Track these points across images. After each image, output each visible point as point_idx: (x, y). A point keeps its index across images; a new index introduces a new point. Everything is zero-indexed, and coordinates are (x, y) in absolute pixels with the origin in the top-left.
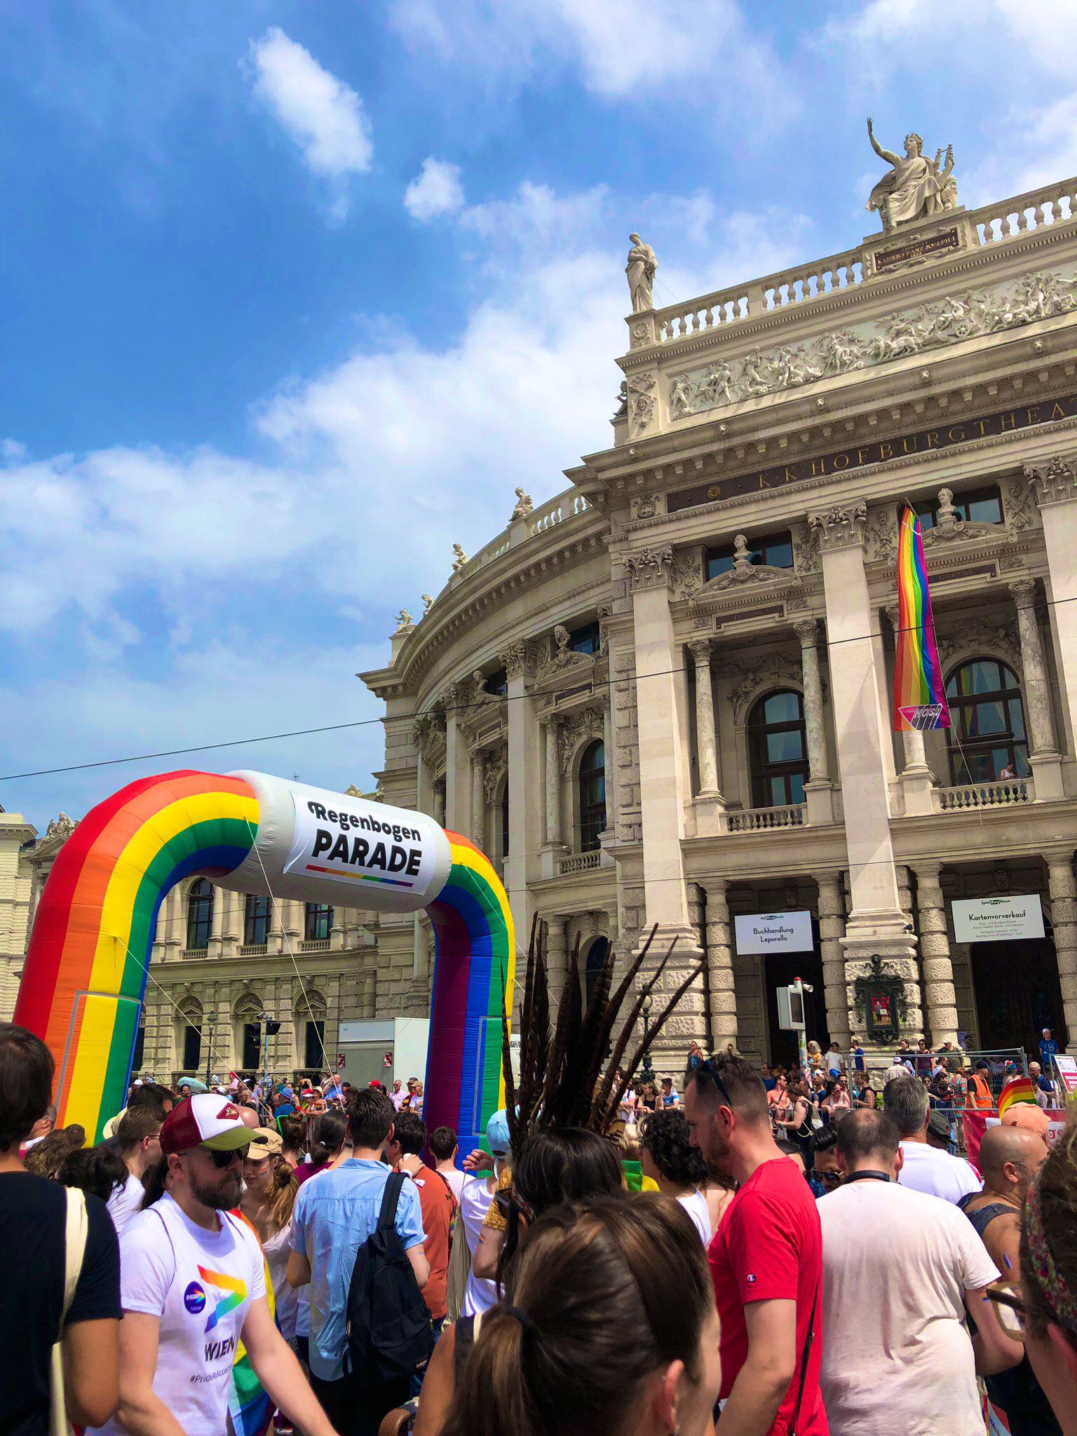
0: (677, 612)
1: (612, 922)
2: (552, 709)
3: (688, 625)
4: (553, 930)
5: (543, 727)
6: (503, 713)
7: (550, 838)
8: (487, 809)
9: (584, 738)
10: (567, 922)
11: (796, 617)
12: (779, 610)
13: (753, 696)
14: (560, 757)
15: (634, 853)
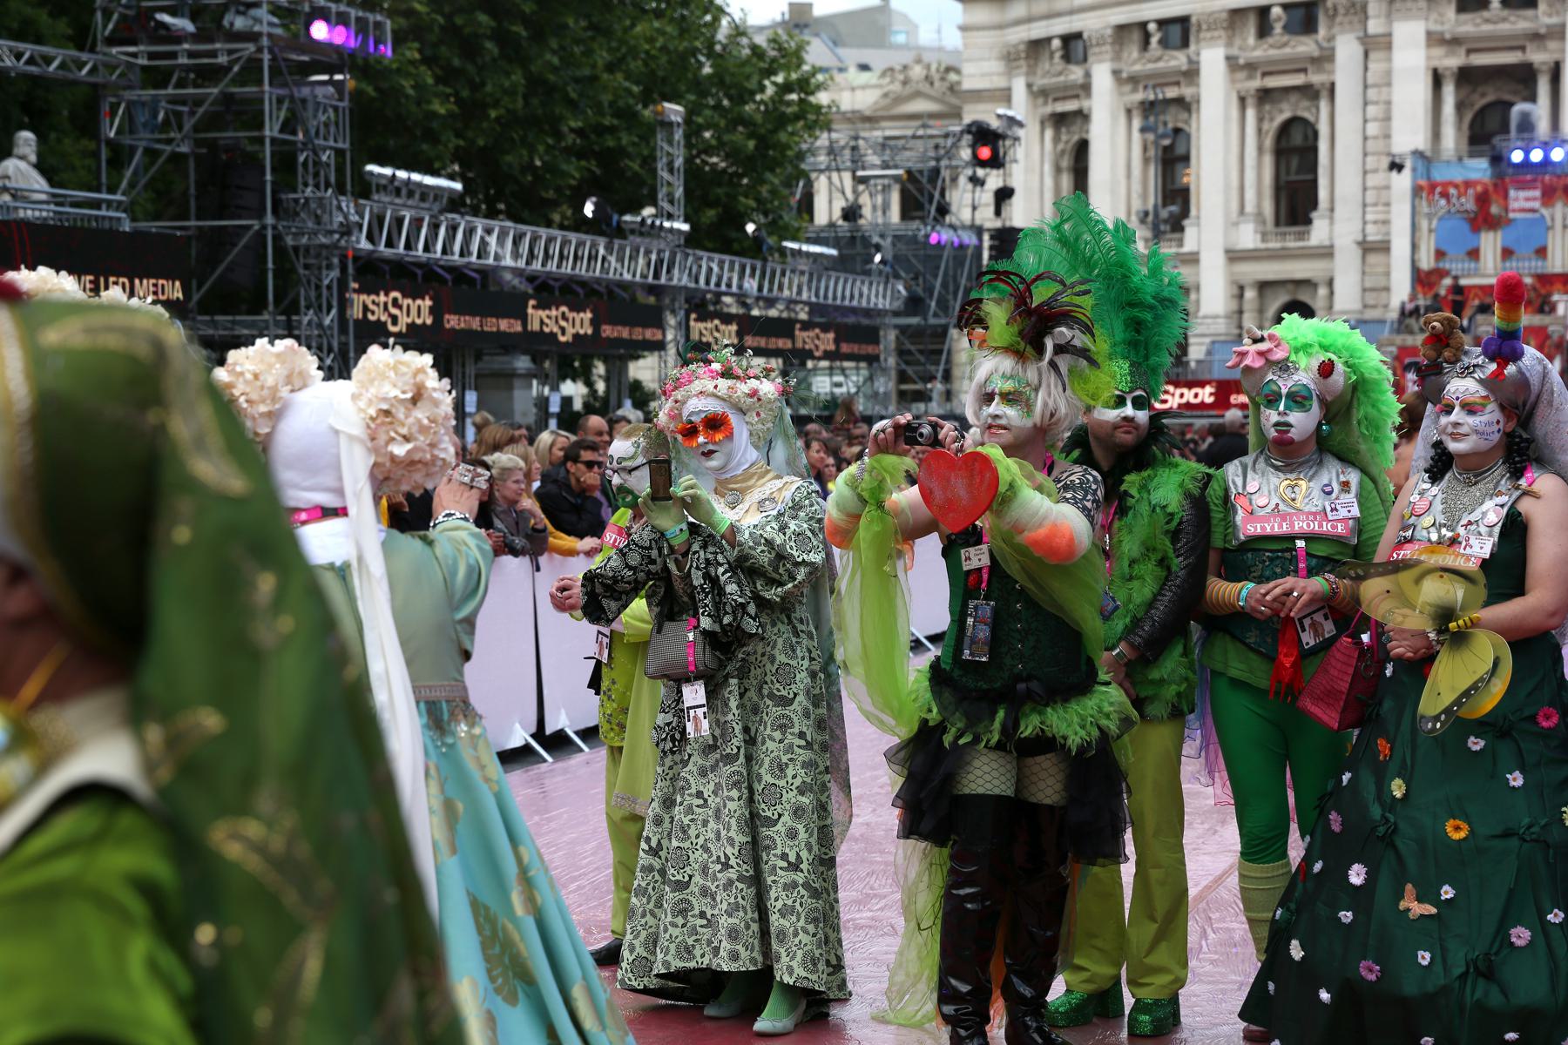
0: (1434, 39)
1: (1322, 291)
2: (1257, 83)
3: (1438, 51)
4: (1250, 294)
5: (1242, 100)
6: (1191, 74)
7: (1250, 207)
8: (1146, 161)
9: (1287, 115)
10: (1264, 286)
11: (1538, 57)
12: (1523, 48)
13: (1477, 107)
14: (1260, 131)
15: (1373, 248)
